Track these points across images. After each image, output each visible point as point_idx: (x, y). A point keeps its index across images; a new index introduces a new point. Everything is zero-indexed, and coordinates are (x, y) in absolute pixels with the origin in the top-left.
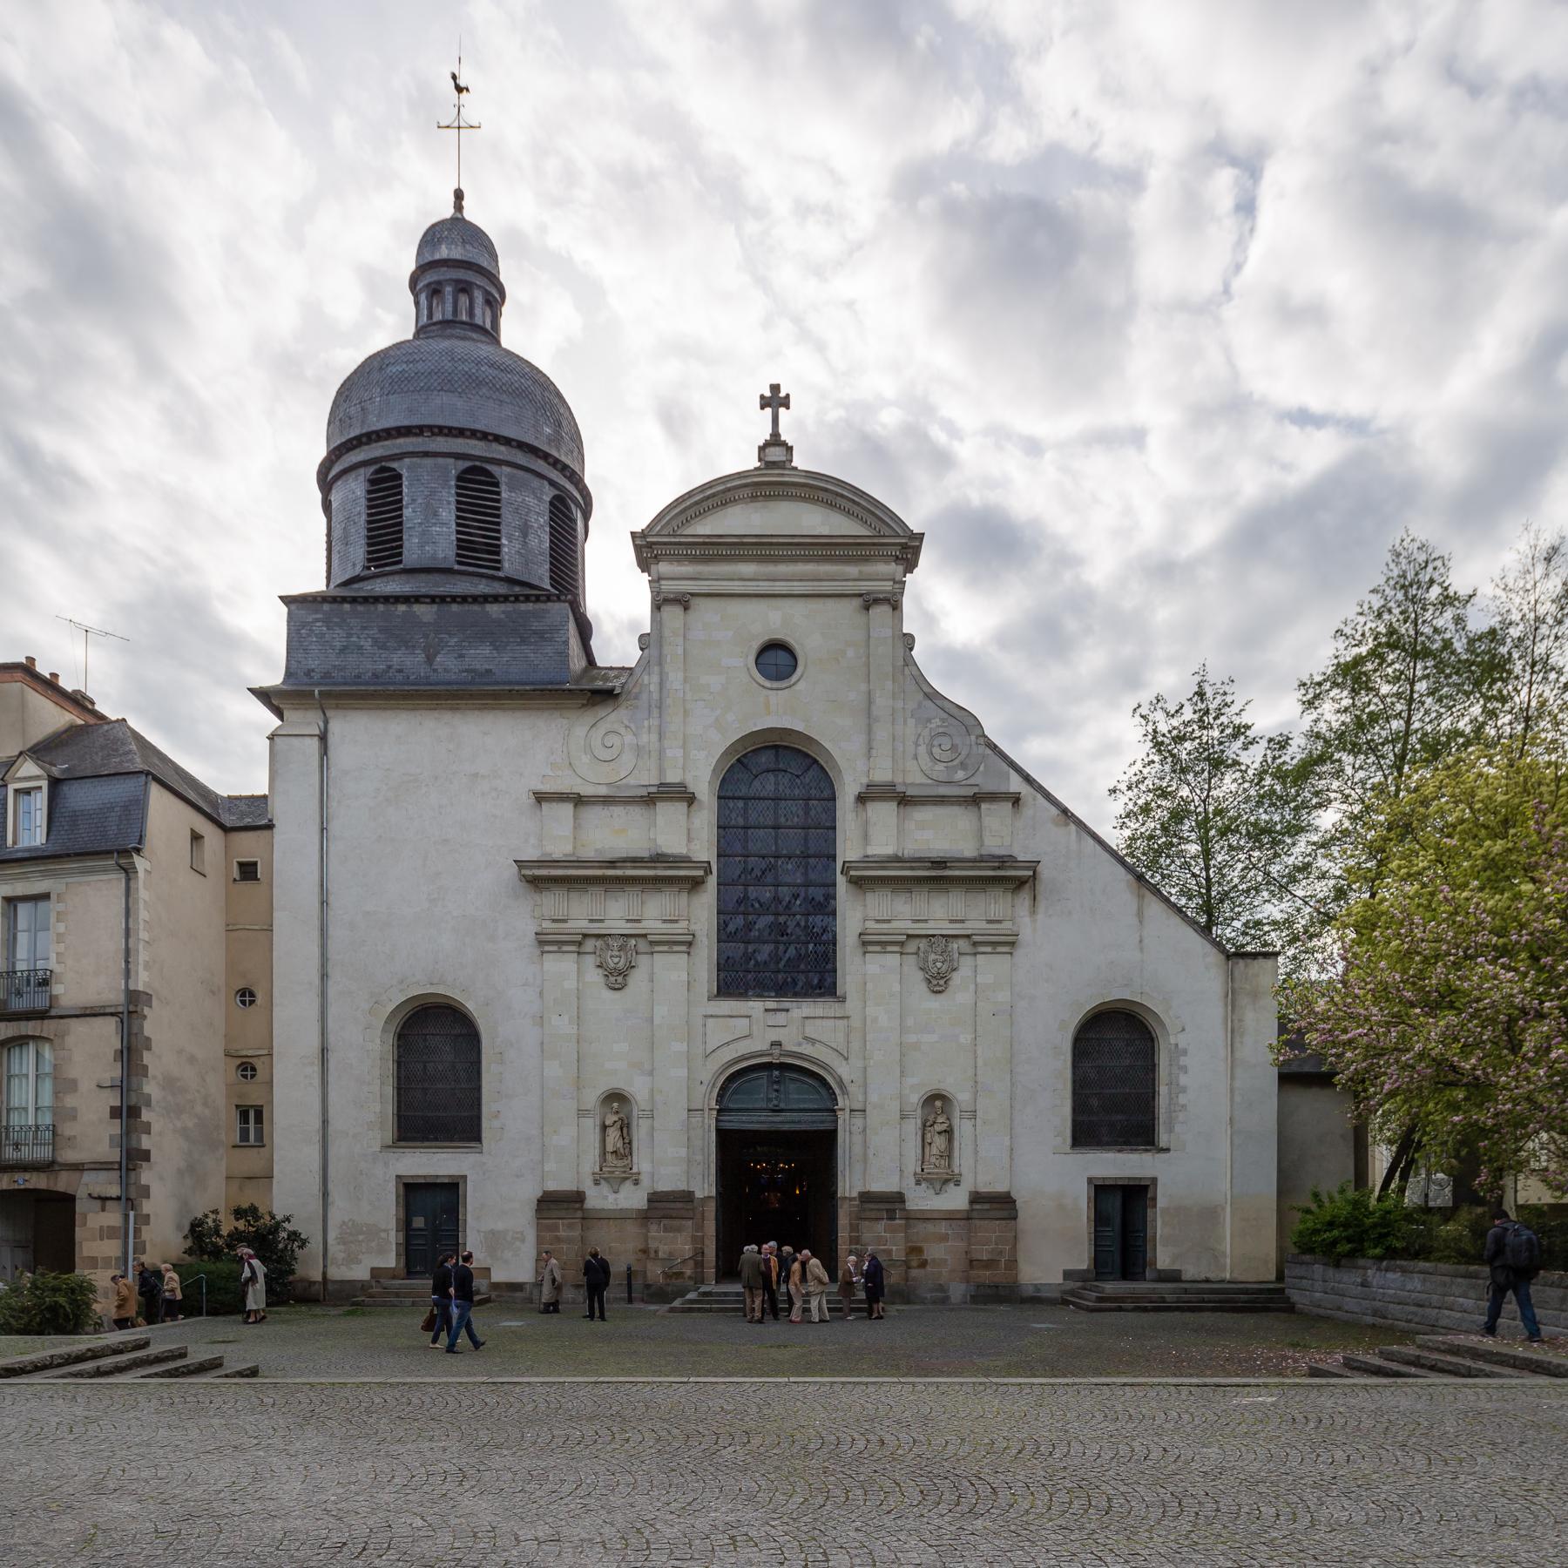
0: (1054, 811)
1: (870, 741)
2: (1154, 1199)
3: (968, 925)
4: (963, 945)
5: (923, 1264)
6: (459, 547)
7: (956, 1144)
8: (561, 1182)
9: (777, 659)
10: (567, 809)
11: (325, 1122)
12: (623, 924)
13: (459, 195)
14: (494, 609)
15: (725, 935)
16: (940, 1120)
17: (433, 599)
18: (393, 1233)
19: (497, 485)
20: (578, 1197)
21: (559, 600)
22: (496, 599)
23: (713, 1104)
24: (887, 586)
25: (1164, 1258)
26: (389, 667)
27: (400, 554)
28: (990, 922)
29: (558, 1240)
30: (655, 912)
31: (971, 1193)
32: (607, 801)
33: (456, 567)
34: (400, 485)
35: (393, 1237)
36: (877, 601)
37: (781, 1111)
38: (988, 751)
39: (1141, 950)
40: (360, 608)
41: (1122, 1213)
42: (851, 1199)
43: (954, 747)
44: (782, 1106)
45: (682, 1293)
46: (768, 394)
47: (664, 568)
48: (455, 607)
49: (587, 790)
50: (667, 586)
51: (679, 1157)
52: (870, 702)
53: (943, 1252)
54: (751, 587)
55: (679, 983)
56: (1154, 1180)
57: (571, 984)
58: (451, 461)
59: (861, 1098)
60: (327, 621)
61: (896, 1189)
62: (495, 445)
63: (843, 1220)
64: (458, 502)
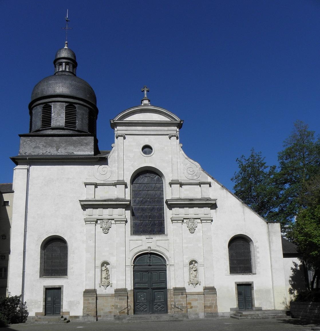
4: (199, 221)
5: (191, 308)
6: (65, 123)
8: (91, 287)
9: (147, 149)
12: (108, 216)
14: (74, 138)
18: (42, 302)
19: (75, 108)
20: (95, 291)
25: (257, 304)
27: (51, 125)
29: (89, 303)
33: (65, 128)
34: (51, 109)
35: (42, 304)
36: (172, 136)
37: (151, 266)
39: (245, 221)
41: (245, 291)
43: (193, 171)
44: (151, 264)
45: (124, 318)
51: (123, 279)
56: (253, 282)
59: (173, 262)
60: (31, 141)
61: (183, 287)
64: (66, 112)
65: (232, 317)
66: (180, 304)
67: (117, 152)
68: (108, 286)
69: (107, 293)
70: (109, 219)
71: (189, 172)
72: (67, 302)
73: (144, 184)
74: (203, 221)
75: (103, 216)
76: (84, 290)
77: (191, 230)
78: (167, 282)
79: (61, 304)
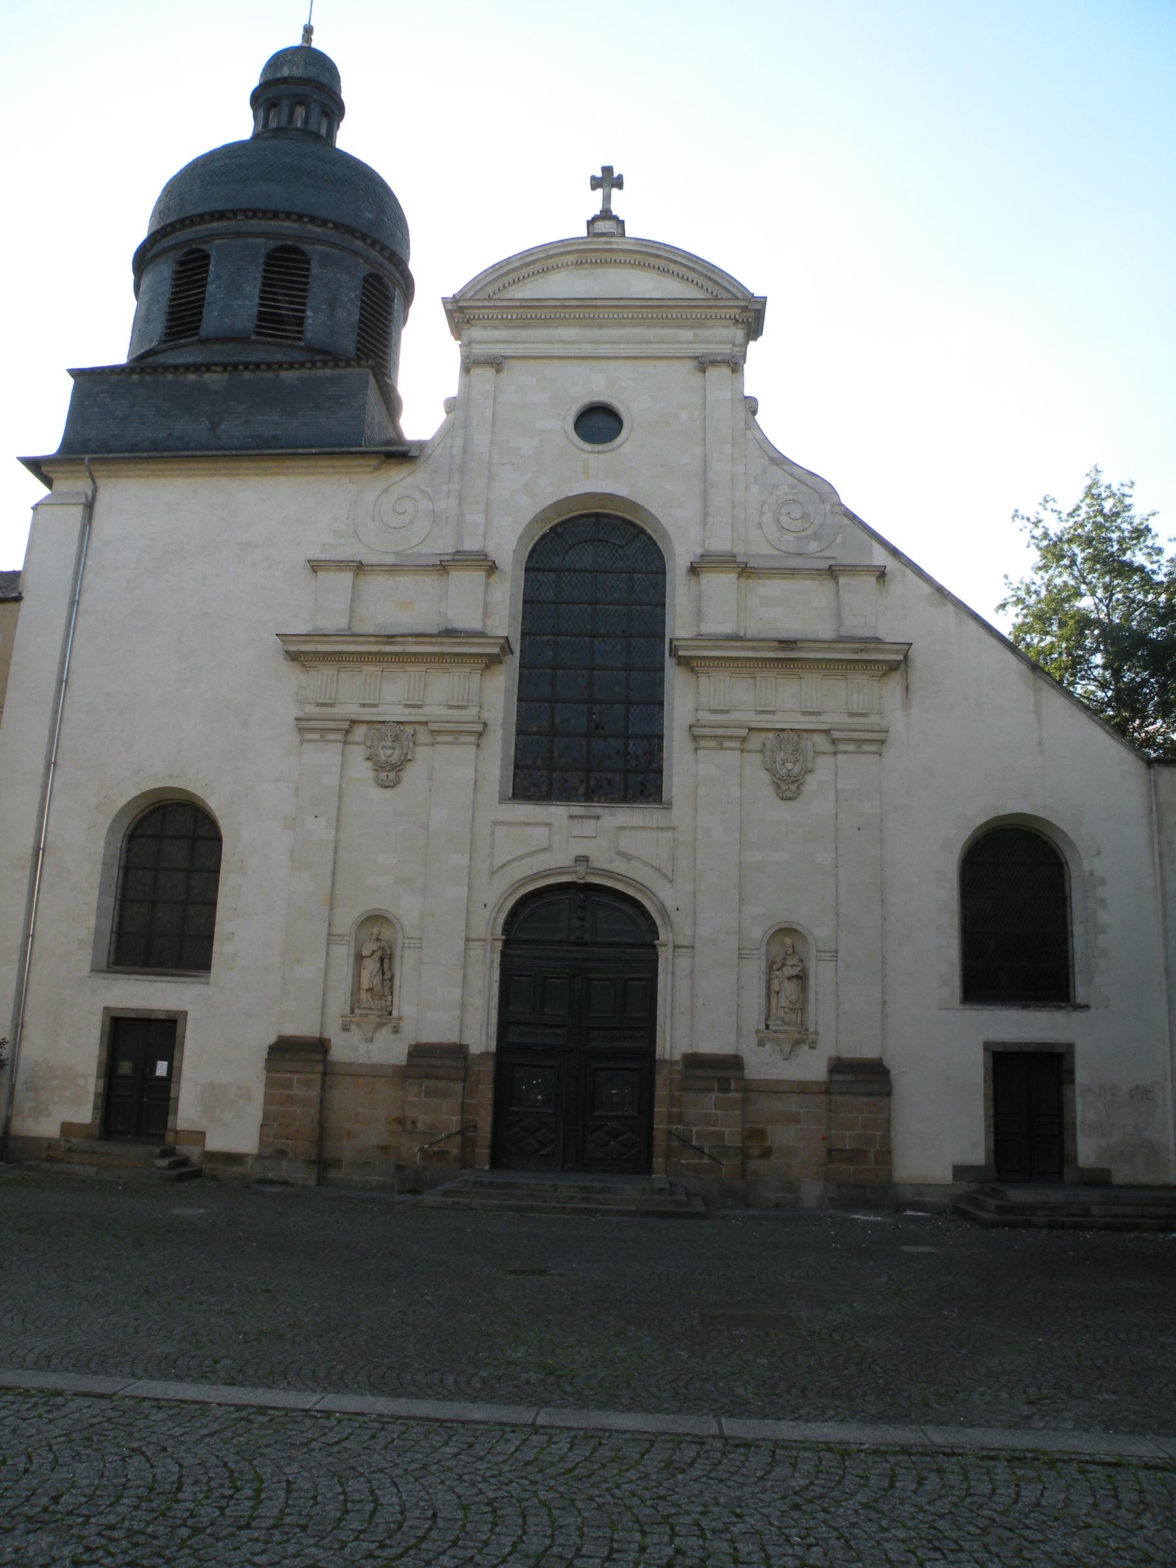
0: (927, 588)
2: (1071, 1072)
5: (766, 1153)
6: (260, 319)
7: (812, 994)
8: (302, 1027)
10: (347, 577)
11: (28, 936)
12: (400, 710)
13: (308, 31)
14: (288, 375)
16: (791, 962)
19: (308, 262)
20: (321, 1046)
24: (726, 349)
25: (1087, 1151)
26: (170, 435)
27: (198, 327)
28: (851, 715)
29: (291, 1100)
31: (830, 1059)
34: (208, 265)
35: (90, 1083)
36: (714, 363)
37: (586, 944)
38: (846, 521)
40: (148, 378)
42: (672, 1063)
43: (805, 516)
44: (587, 938)
46: (599, 174)
47: (476, 333)
50: (478, 350)
51: (452, 999)
52: (706, 466)
53: (796, 1141)
54: (573, 350)
55: (466, 777)
57: (331, 780)
63: (661, 1092)
65: (957, 1211)
66: (714, 1133)
69: (373, 1061)
72: (199, 1088)
73: (580, 571)
74: (842, 747)
75: (380, 710)
76: (273, 1039)
77: (784, 787)
78: (658, 1028)
79: (172, 1095)
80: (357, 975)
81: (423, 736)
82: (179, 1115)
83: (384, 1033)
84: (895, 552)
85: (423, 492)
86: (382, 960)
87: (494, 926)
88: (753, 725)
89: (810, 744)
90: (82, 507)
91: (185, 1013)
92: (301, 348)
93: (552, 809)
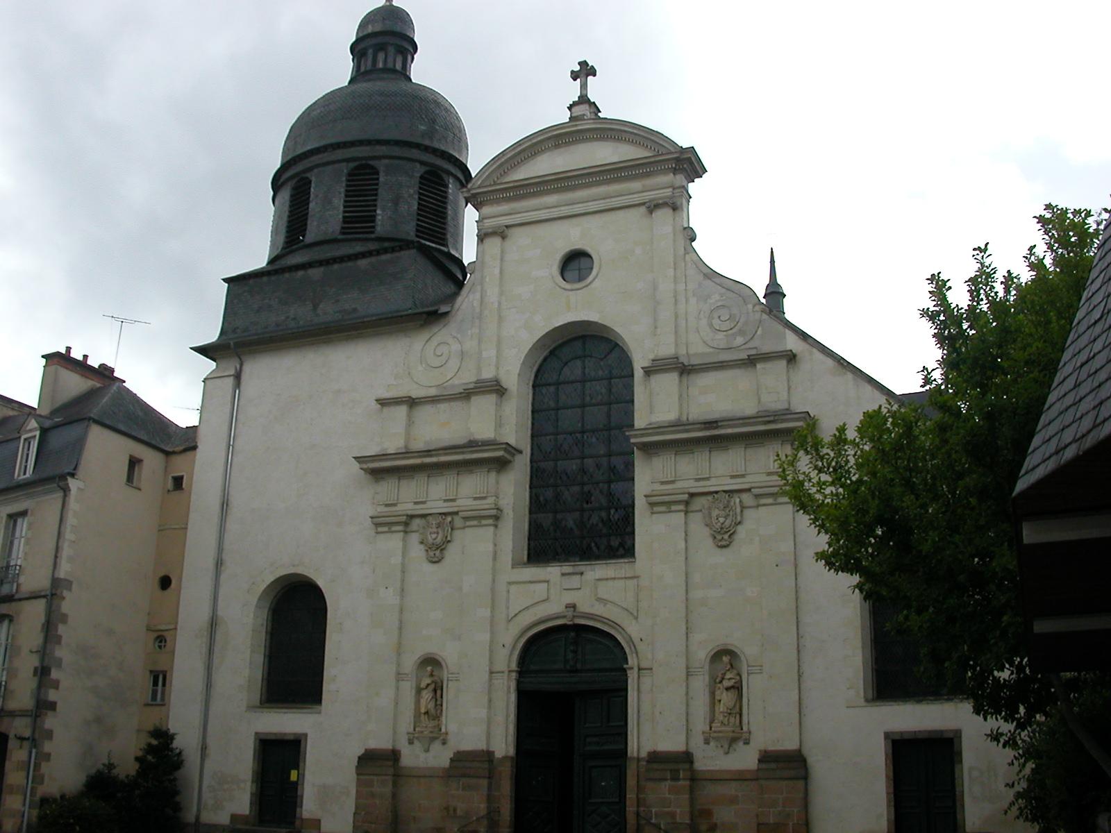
1: (655, 320)
3: (749, 479)
8: (380, 742)
10: (403, 409)
11: (209, 685)
12: (441, 504)
14: (363, 263)
15: (536, 505)
16: (728, 676)
17: (321, 263)
19: (377, 173)
20: (394, 755)
21: (409, 248)
22: (363, 255)
23: (514, 666)
24: (668, 192)
30: (468, 490)
32: (434, 400)
33: (341, 237)
37: (576, 671)
40: (273, 278)
42: (639, 759)
44: (579, 666)
46: (577, 68)
47: (487, 210)
48: (336, 266)
49: (416, 393)
51: (483, 718)
54: (556, 213)
57: (396, 560)
58: (344, 164)
61: (682, 748)
62: (378, 147)
63: (631, 782)
67: (479, 288)
68: (433, 739)
69: (429, 765)
70: (445, 514)
71: (716, 322)
75: (429, 504)
76: (361, 752)
77: (719, 537)
78: (629, 733)
79: (299, 793)
80: (418, 702)
81: (458, 522)
82: (304, 807)
83: (436, 746)
84: (804, 336)
85: (454, 337)
86: (435, 691)
87: (509, 661)
88: (692, 490)
89: (738, 500)
90: (232, 378)
91: (306, 735)
92: (372, 239)
93: (549, 569)
